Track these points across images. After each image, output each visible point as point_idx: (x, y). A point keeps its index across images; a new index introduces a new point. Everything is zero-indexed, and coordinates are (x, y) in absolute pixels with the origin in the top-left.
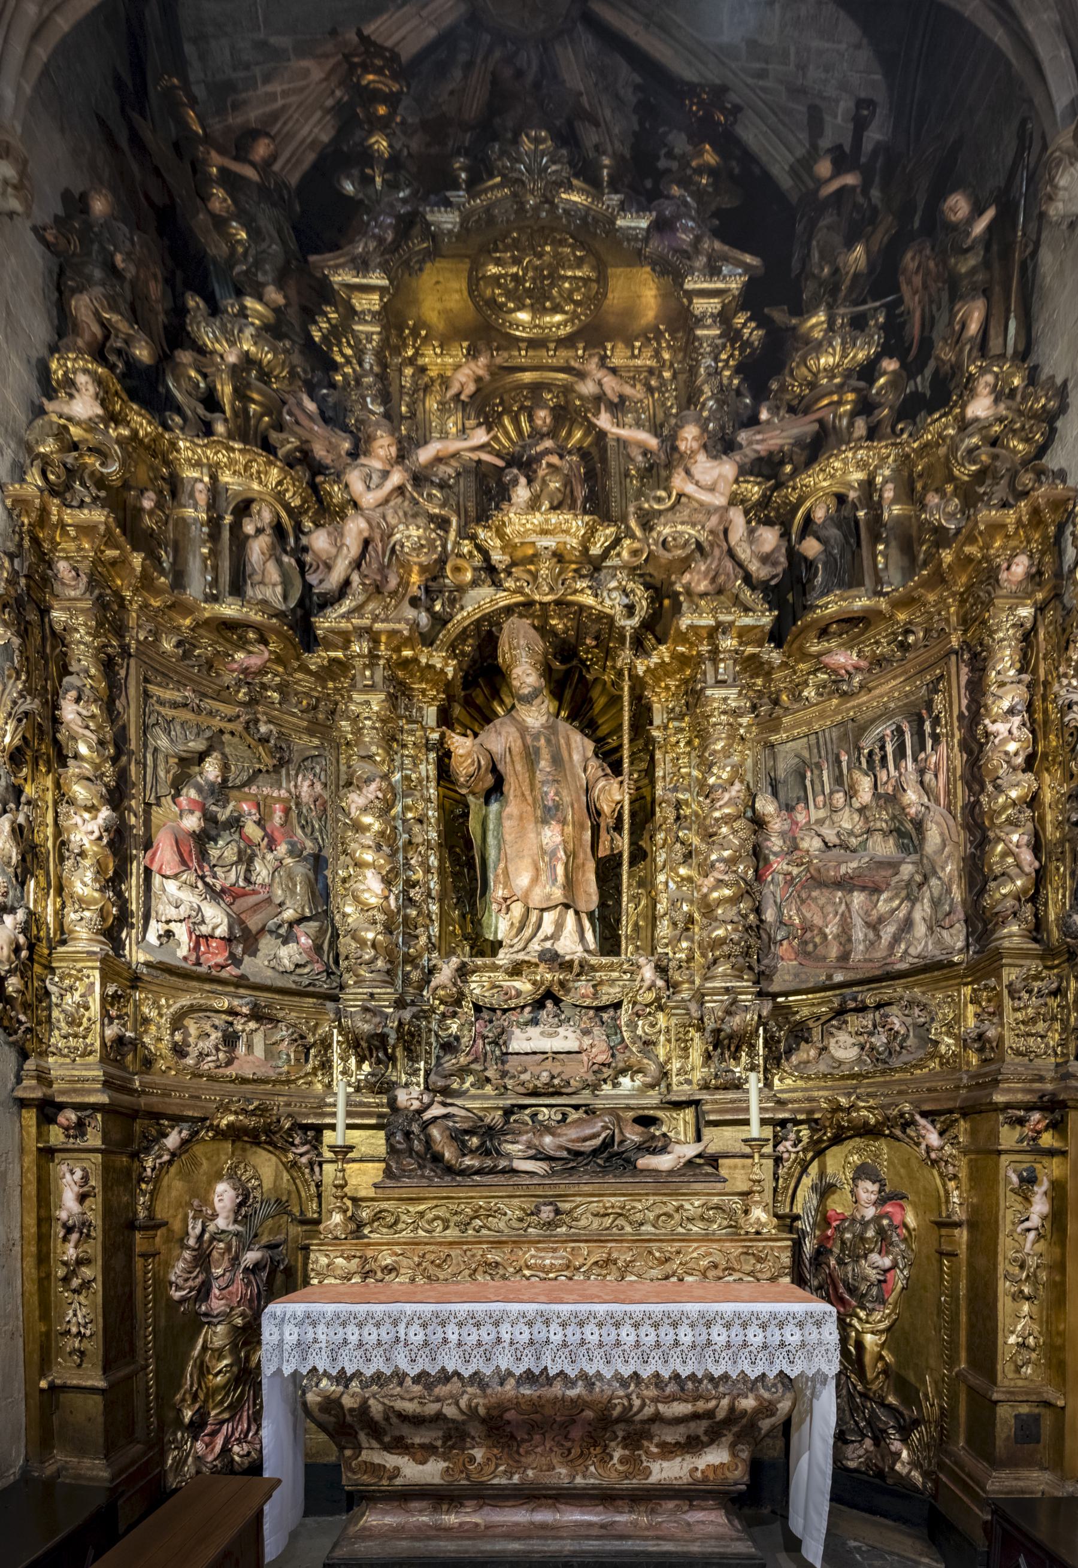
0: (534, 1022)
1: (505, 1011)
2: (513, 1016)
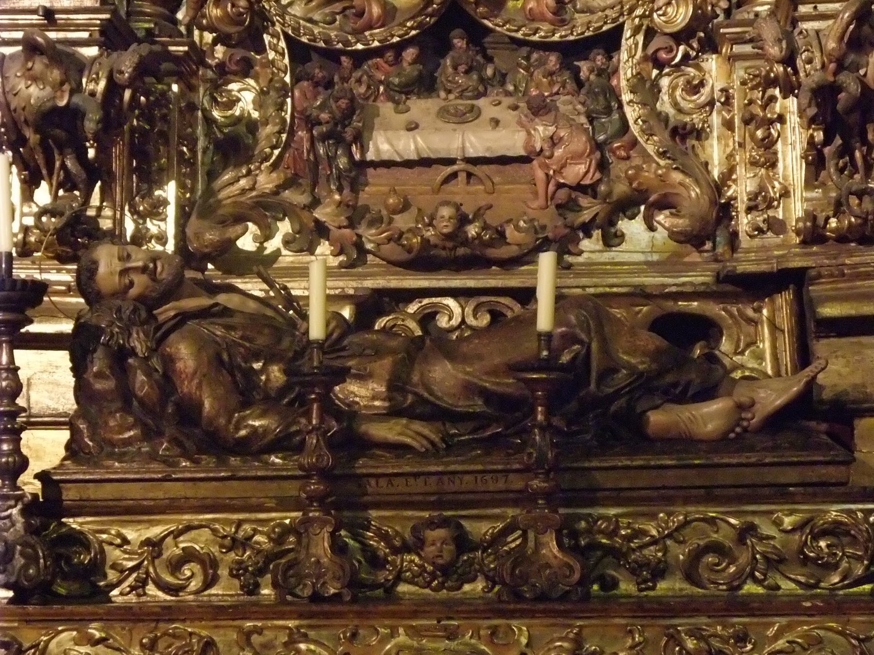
0: (425, 84)
1: (359, 58)
2: (380, 70)
